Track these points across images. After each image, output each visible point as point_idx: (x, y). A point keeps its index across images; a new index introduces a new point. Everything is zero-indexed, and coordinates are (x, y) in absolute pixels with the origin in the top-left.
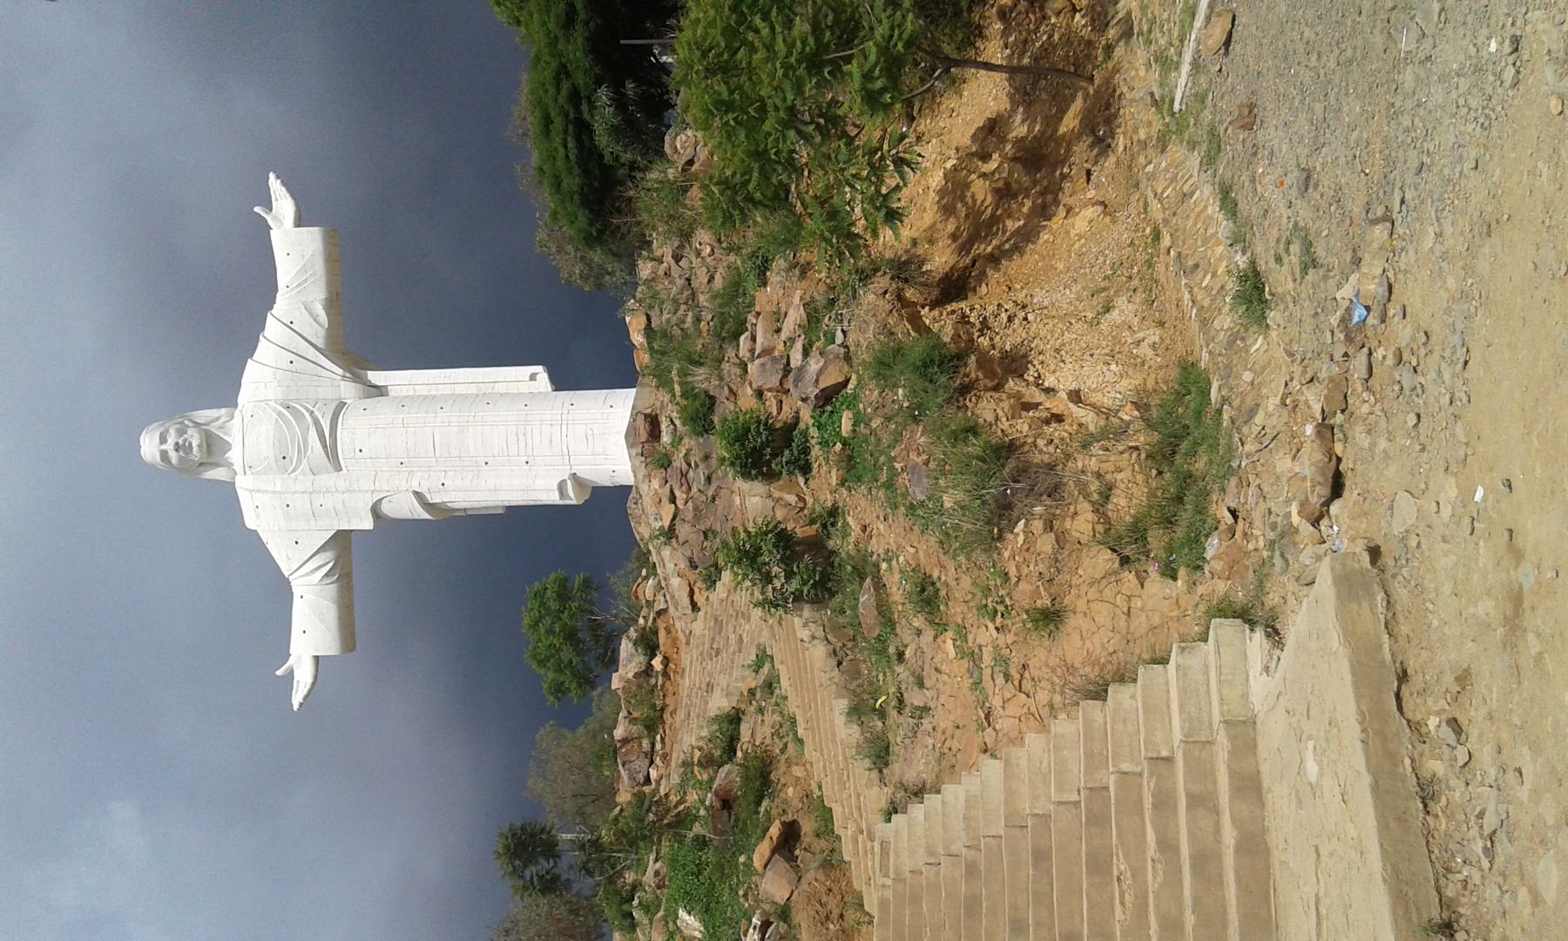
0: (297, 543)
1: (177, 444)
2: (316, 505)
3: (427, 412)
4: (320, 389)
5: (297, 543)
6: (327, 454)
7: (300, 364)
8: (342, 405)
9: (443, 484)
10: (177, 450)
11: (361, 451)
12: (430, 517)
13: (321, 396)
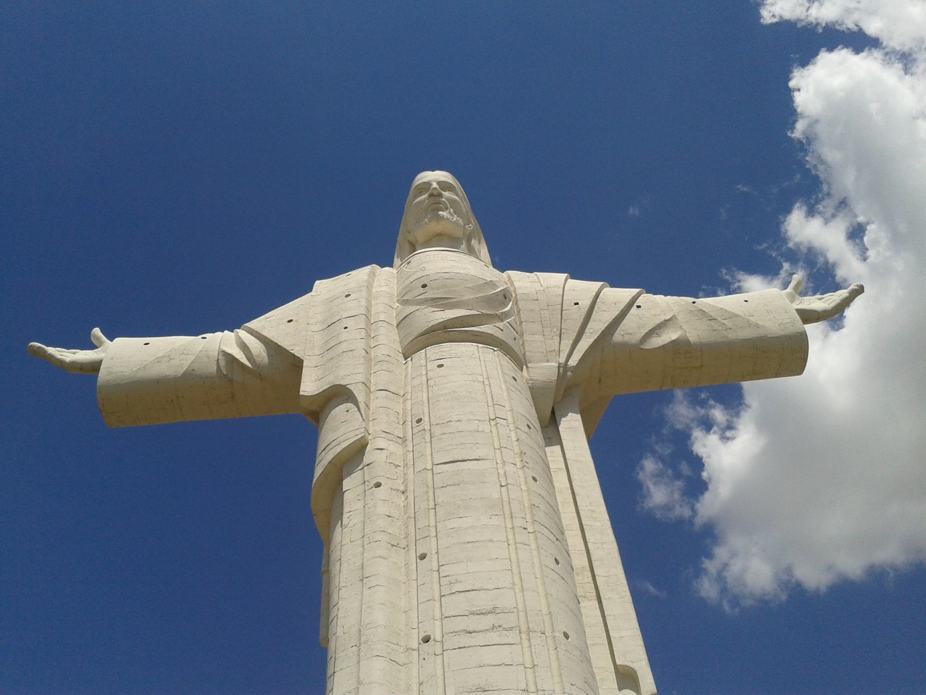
0: (290, 321)
1: (440, 195)
2: (350, 323)
3: (522, 453)
4: (539, 337)
5: (290, 321)
6: (432, 330)
7: (577, 316)
8: (520, 362)
9: (378, 485)
10: (431, 195)
11: (441, 366)
12: (318, 471)
13: (526, 337)
